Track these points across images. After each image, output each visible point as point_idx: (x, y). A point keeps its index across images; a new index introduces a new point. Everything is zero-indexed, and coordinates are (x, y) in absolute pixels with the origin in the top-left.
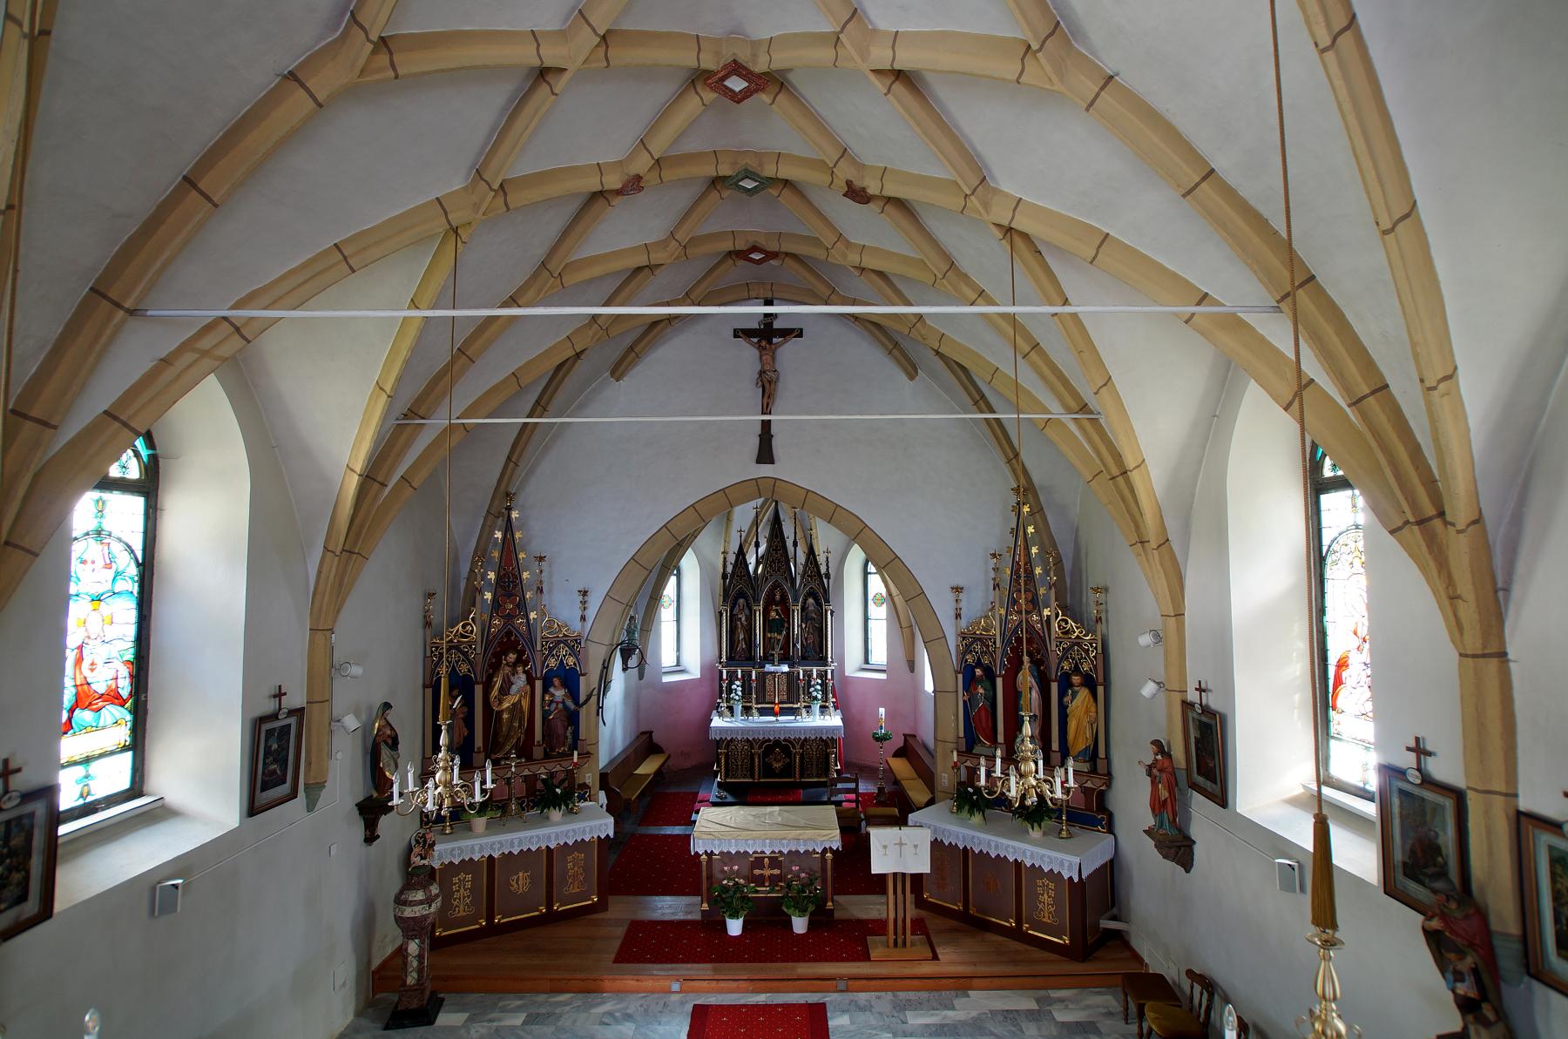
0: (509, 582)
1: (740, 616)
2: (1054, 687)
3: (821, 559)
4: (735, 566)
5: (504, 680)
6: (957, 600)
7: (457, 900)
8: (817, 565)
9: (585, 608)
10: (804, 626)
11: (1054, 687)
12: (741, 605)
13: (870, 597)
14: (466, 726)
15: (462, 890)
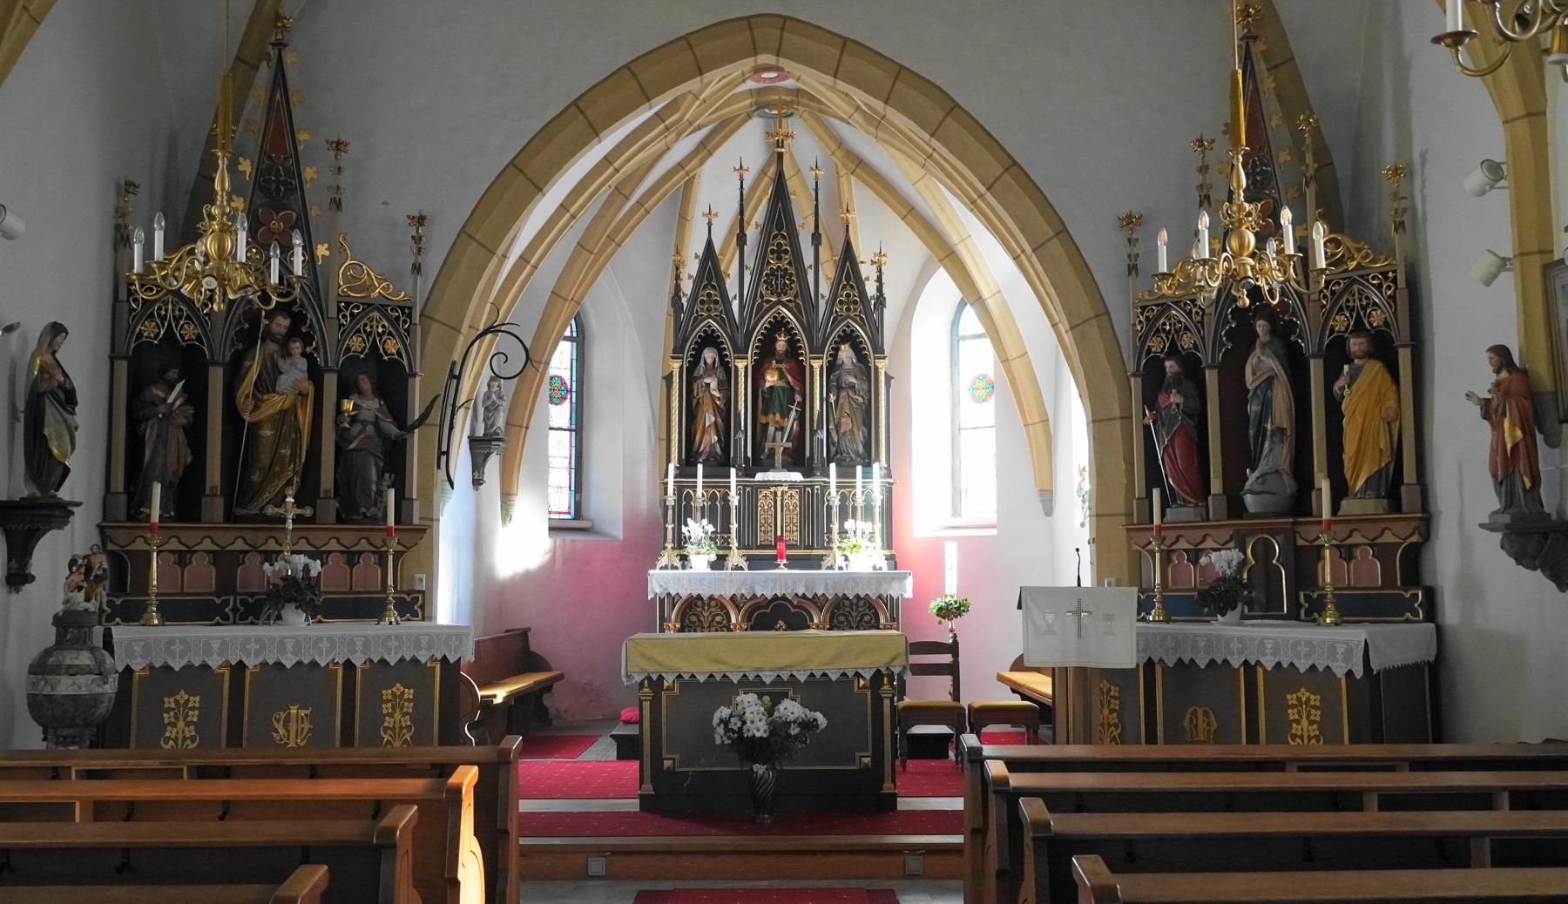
0: (278, 182)
1: (707, 380)
2: (1316, 368)
3: (867, 271)
5: (264, 366)
6: (1129, 240)
8: (860, 285)
9: (419, 250)
10: (832, 398)
11: (1316, 368)
12: (709, 361)
14: (190, 445)
15: (181, 725)
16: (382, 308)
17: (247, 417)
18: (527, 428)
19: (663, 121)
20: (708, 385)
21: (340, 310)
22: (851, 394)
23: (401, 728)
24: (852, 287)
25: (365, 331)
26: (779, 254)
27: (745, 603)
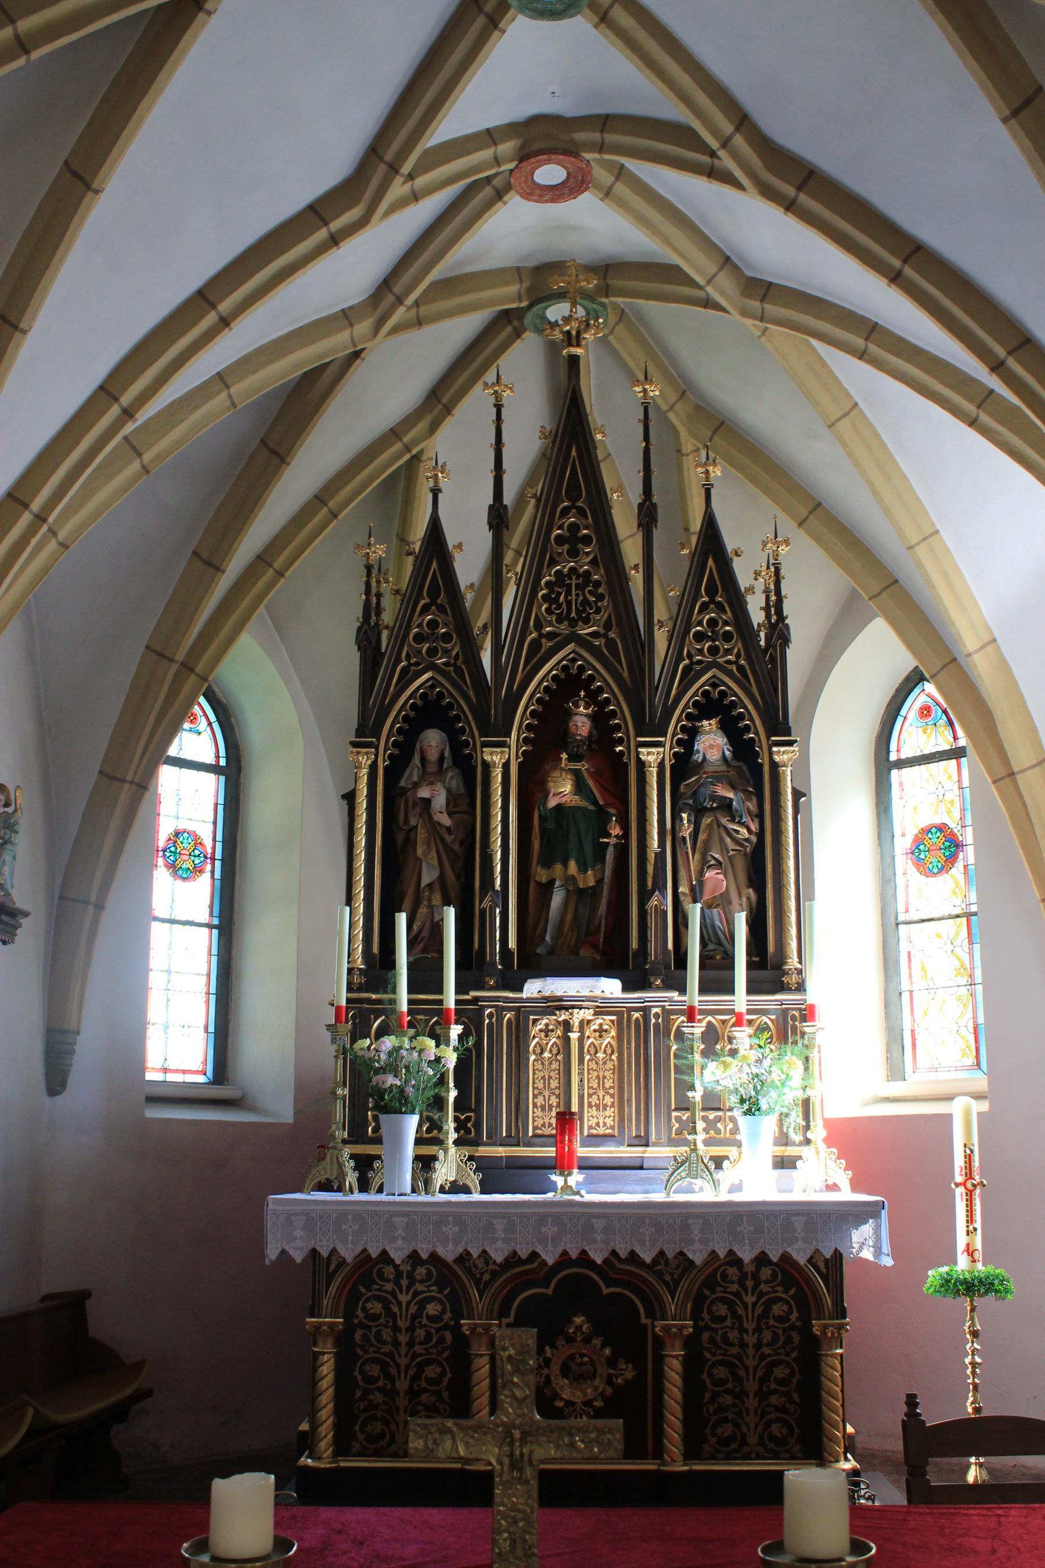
1: (424, 793)
4: (410, 599)
8: (736, 600)
10: (686, 830)
12: (433, 755)
13: (902, 844)
18: (100, 907)
19: (326, 224)
20: (427, 802)
22: (724, 821)
24: (720, 608)
26: (573, 542)
27: (495, 1275)
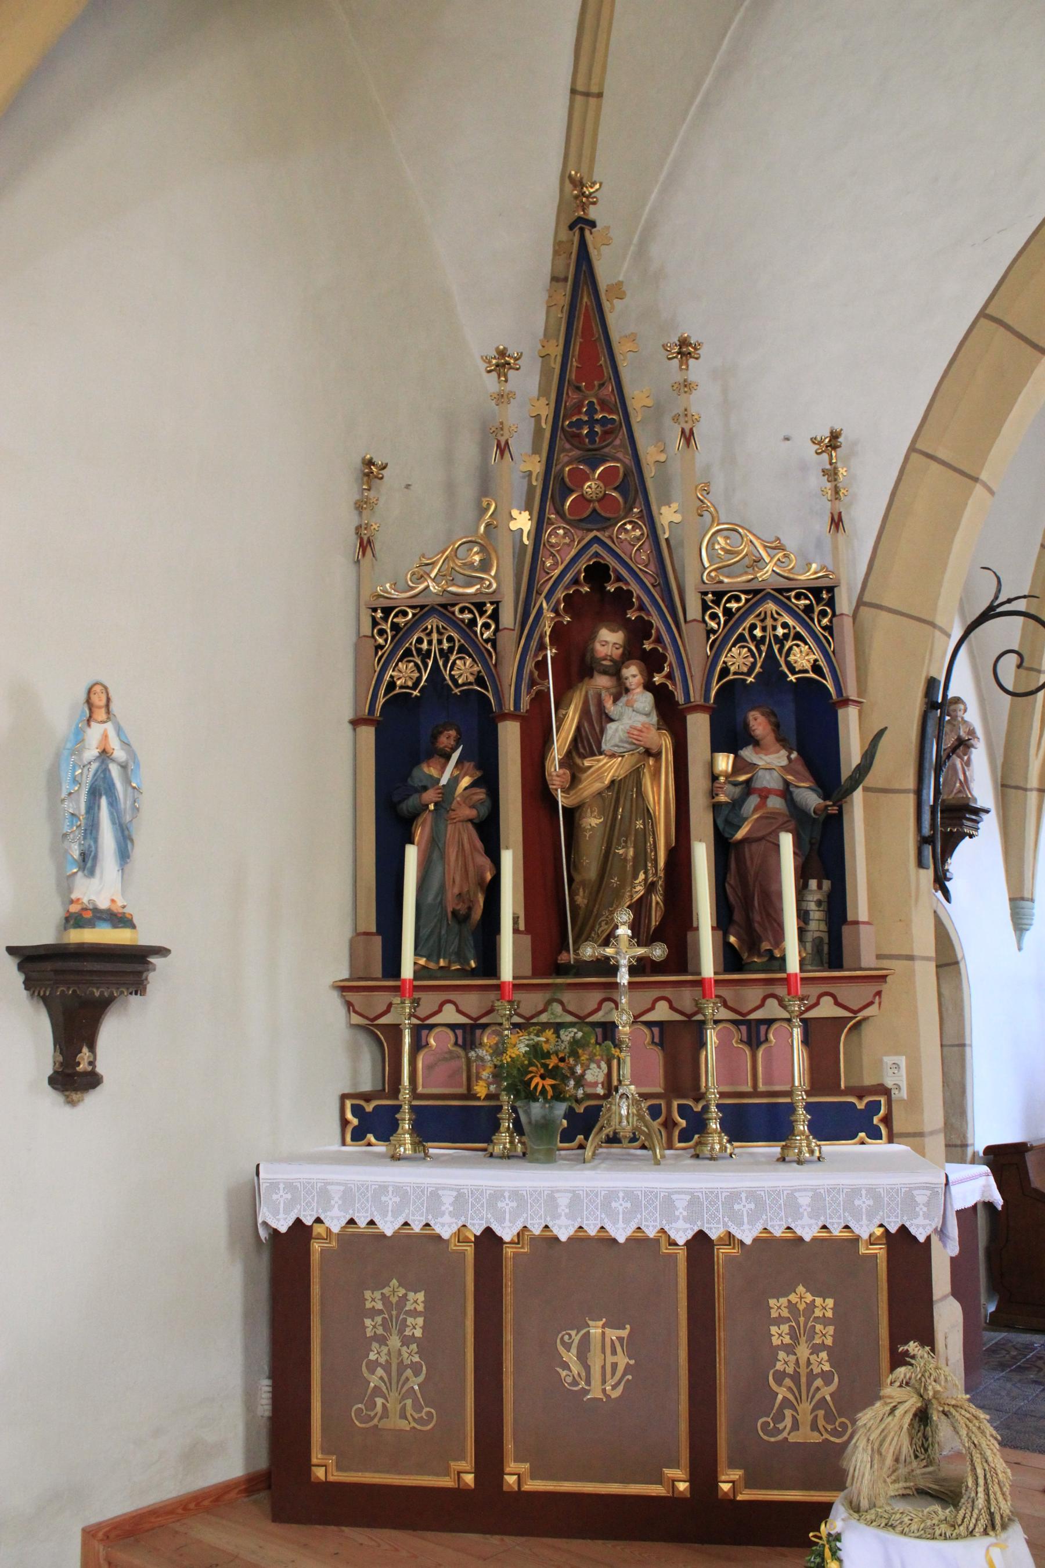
5: (585, 713)
7: (380, 1372)
9: (836, 491)
15: (395, 1341)
16: (780, 594)
17: (562, 800)
21: (705, 607)
23: (811, 1377)
25: (753, 637)
